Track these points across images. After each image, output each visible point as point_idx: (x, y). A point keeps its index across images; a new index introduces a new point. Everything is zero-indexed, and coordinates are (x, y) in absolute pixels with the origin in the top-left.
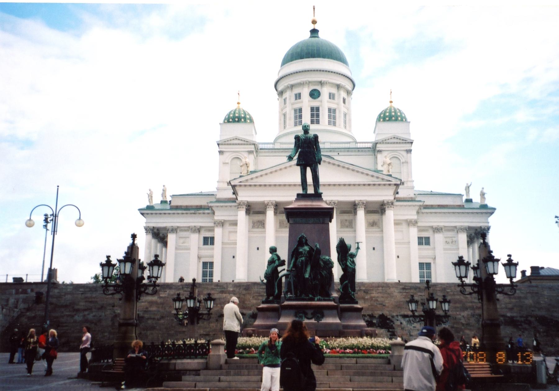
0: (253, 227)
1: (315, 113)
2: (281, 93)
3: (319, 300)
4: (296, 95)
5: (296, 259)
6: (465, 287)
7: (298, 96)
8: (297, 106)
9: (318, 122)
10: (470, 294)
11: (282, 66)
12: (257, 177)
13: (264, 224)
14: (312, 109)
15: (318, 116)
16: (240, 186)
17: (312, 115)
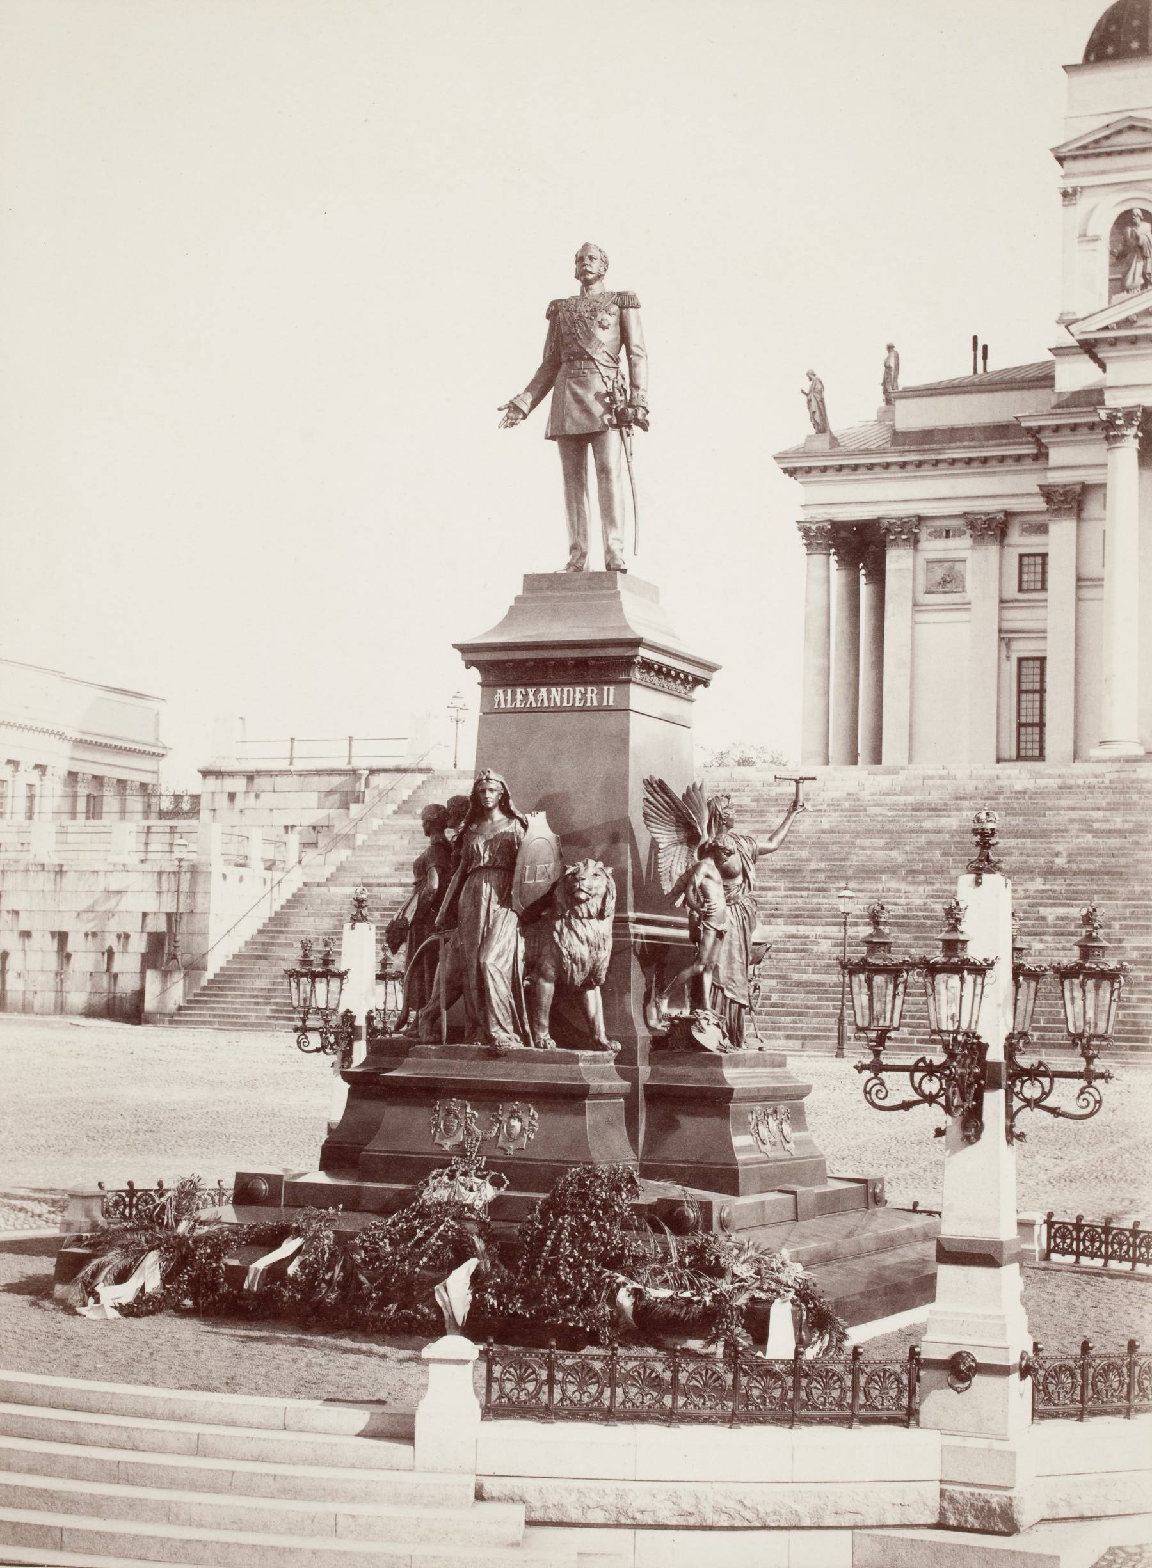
6: (884, 1075)
10: (906, 1106)
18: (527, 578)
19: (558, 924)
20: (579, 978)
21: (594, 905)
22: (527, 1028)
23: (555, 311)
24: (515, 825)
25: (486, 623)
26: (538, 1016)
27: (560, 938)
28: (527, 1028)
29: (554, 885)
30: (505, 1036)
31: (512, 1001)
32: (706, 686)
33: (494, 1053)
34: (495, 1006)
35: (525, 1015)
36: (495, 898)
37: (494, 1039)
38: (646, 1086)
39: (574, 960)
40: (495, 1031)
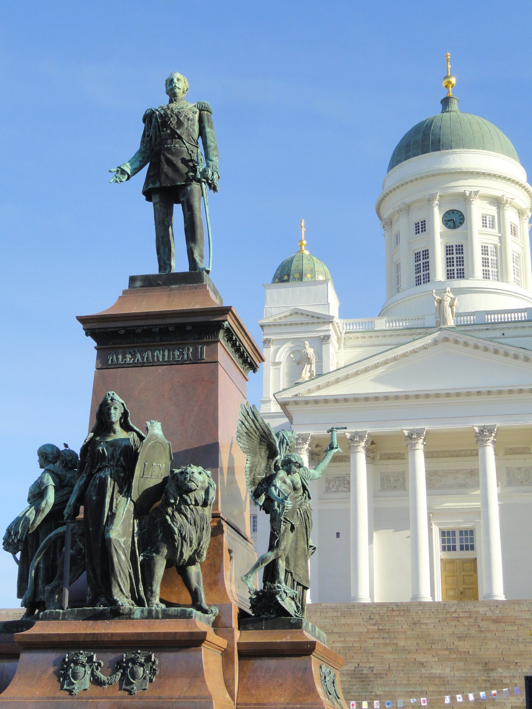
0: (328, 490)
1: (455, 256)
2: (388, 224)
3: (150, 615)
4: (417, 224)
5: (90, 476)
7: (422, 227)
8: (420, 248)
9: (461, 275)
11: (388, 171)
12: (328, 385)
13: (349, 482)
14: (449, 250)
15: (461, 261)
16: (296, 403)
17: (449, 262)
18: (133, 279)
19: (170, 510)
20: (187, 554)
21: (200, 495)
22: (142, 593)
23: (149, 118)
24: (132, 436)
25: (105, 301)
26: (152, 586)
27: (172, 521)
28: (142, 593)
29: (165, 480)
30: (124, 601)
31: (131, 571)
32: (254, 372)
33: (115, 613)
34: (118, 574)
35: (141, 583)
36: (117, 489)
37: (116, 602)
38: (238, 644)
39: (183, 538)
40: (117, 595)
